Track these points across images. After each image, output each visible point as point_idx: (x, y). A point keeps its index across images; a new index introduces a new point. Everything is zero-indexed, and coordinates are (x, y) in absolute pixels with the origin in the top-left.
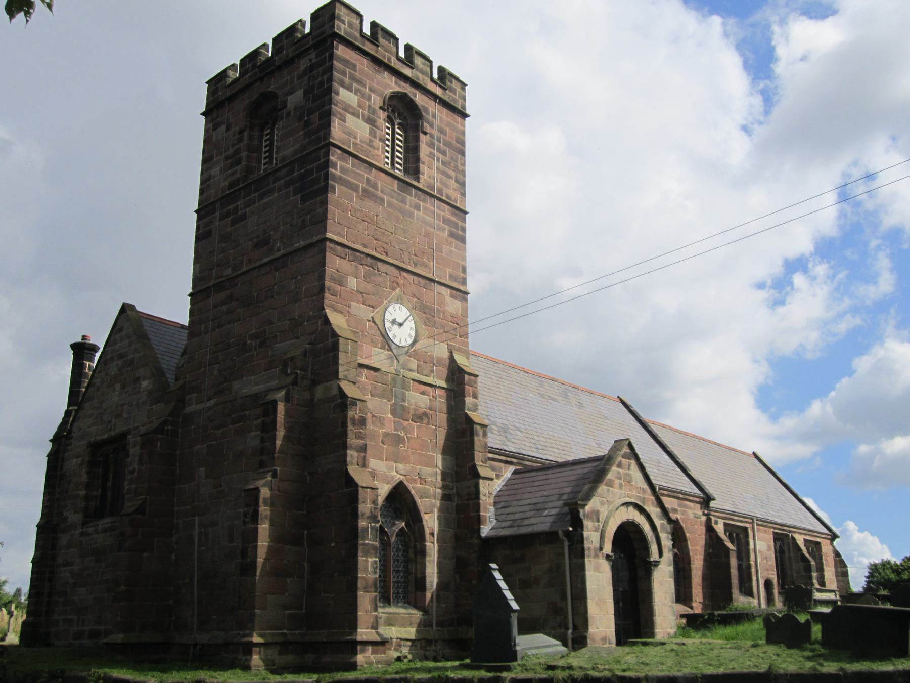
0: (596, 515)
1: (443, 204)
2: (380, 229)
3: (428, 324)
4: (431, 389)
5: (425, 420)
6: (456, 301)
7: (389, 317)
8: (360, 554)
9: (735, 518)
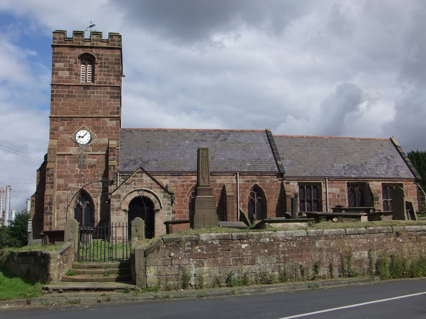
0: (119, 196)
1: (107, 87)
3: (98, 133)
4: (98, 156)
5: (94, 167)
7: (77, 135)
8: (45, 215)
9: (307, 179)
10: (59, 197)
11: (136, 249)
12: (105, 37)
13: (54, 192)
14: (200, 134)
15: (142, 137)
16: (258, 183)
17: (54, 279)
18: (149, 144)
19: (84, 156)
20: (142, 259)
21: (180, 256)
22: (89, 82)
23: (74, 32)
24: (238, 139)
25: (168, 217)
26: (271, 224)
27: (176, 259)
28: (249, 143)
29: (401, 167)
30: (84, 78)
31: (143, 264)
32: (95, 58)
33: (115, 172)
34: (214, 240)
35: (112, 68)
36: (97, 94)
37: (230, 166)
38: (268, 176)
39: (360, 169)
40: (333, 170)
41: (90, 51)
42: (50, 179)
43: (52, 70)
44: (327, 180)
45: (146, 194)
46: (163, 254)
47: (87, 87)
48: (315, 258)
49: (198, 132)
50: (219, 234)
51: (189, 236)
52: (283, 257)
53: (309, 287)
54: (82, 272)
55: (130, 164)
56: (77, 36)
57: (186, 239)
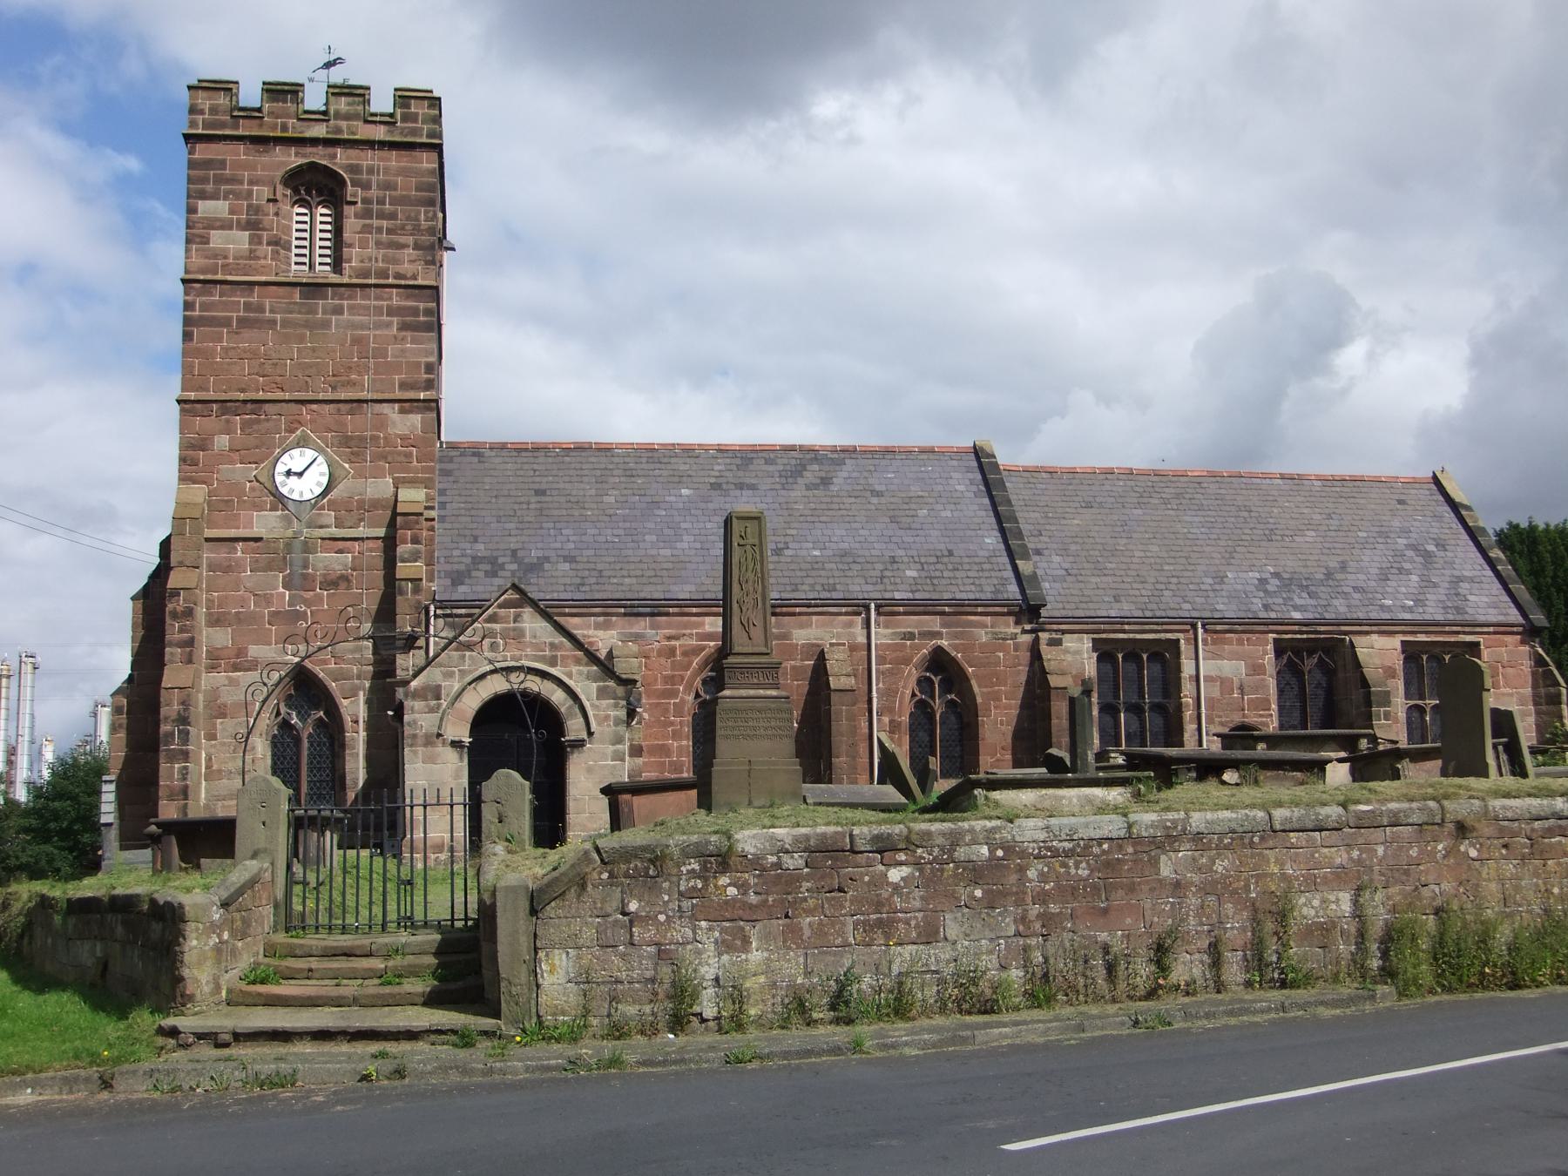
0: (436, 693)
2: (270, 362)
4: (356, 544)
5: (343, 585)
6: (411, 415)
7: (281, 468)
9: (1126, 627)
10: (214, 694)
11: (498, 885)
12: (382, 102)
13: (197, 676)
14: (734, 461)
15: (518, 473)
16: (944, 643)
17: (198, 997)
18: (544, 499)
19: (305, 543)
20: (522, 922)
21: (661, 913)
22: (323, 271)
23: (265, 87)
24: (871, 481)
25: (614, 766)
26: (996, 795)
27: (648, 924)
28: (912, 494)
29: (1471, 580)
30: (305, 255)
31: (524, 942)
32: (342, 182)
33: (419, 602)
34: (787, 852)
35: (408, 218)
36: (354, 315)
37: (842, 580)
38: (984, 618)
39: (1323, 589)
40: (1224, 593)
41: (325, 156)
42: (181, 631)
43: (188, 227)
44: (1200, 631)
45: (534, 685)
46: (599, 905)
47: (314, 289)
48: (1156, 919)
49: (725, 455)
50: (803, 830)
51: (695, 838)
52: (1039, 916)
53: (1136, 1023)
54: (304, 970)
55: (474, 573)
56: (277, 101)
57: (683, 850)
